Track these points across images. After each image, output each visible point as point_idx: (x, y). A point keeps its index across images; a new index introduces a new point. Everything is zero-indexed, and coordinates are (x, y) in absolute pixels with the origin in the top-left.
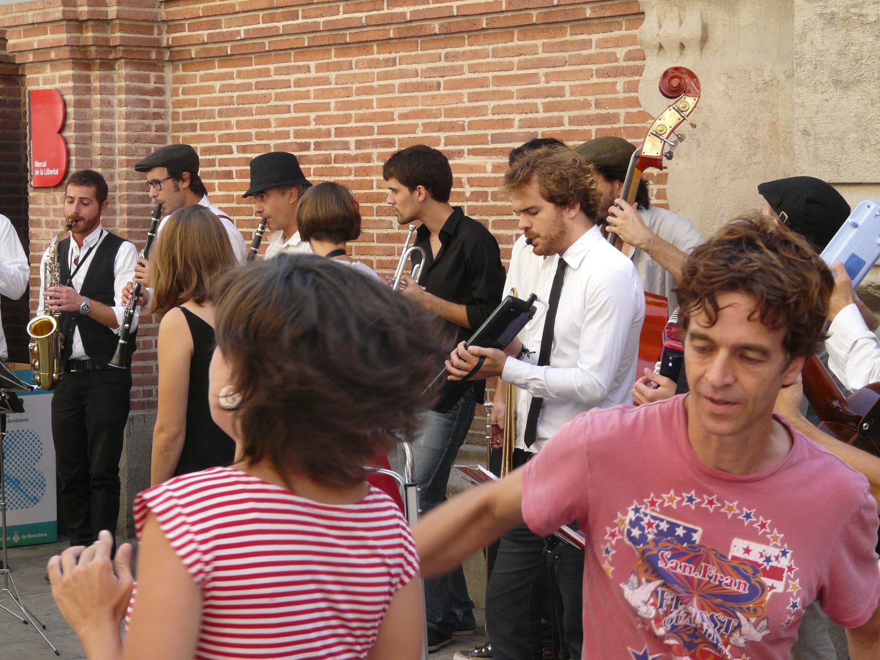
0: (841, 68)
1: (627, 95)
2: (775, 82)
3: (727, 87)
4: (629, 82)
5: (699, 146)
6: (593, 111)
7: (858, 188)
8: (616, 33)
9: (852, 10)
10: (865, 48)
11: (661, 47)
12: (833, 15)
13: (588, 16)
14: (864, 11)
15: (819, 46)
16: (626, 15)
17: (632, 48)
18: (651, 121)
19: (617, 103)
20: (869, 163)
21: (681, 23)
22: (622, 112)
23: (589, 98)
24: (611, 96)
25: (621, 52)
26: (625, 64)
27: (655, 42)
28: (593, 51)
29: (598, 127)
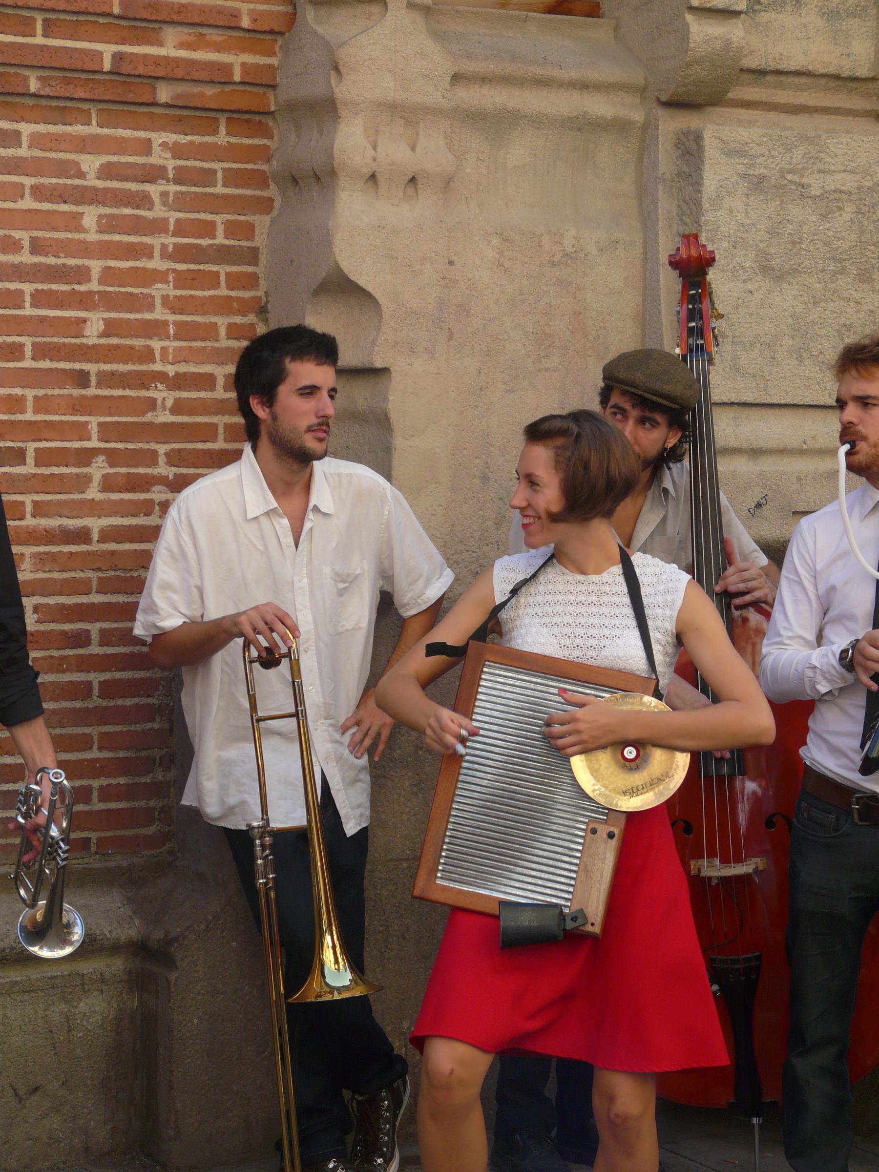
0: (773, 251)
1: (106, 237)
2: (582, 255)
3: (501, 253)
4: (111, 217)
5: (450, 338)
6: (25, 257)
7: (783, 410)
8: (79, 129)
9: (789, 177)
10: (806, 229)
11: (373, 176)
12: (762, 178)
13: (33, 90)
14: (804, 180)
15: (741, 217)
16: (100, 101)
17: (115, 159)
18: (159, 286)
19: (84, 249)
20: (808, 378)
21: (413, 149)
22: (96, 266)
23: (16, 234)
24: (69, 235)
25: (91, 163)
26: (100, 184)
27: (367, 171)
28: (23, 152)
29: (40, 286)
